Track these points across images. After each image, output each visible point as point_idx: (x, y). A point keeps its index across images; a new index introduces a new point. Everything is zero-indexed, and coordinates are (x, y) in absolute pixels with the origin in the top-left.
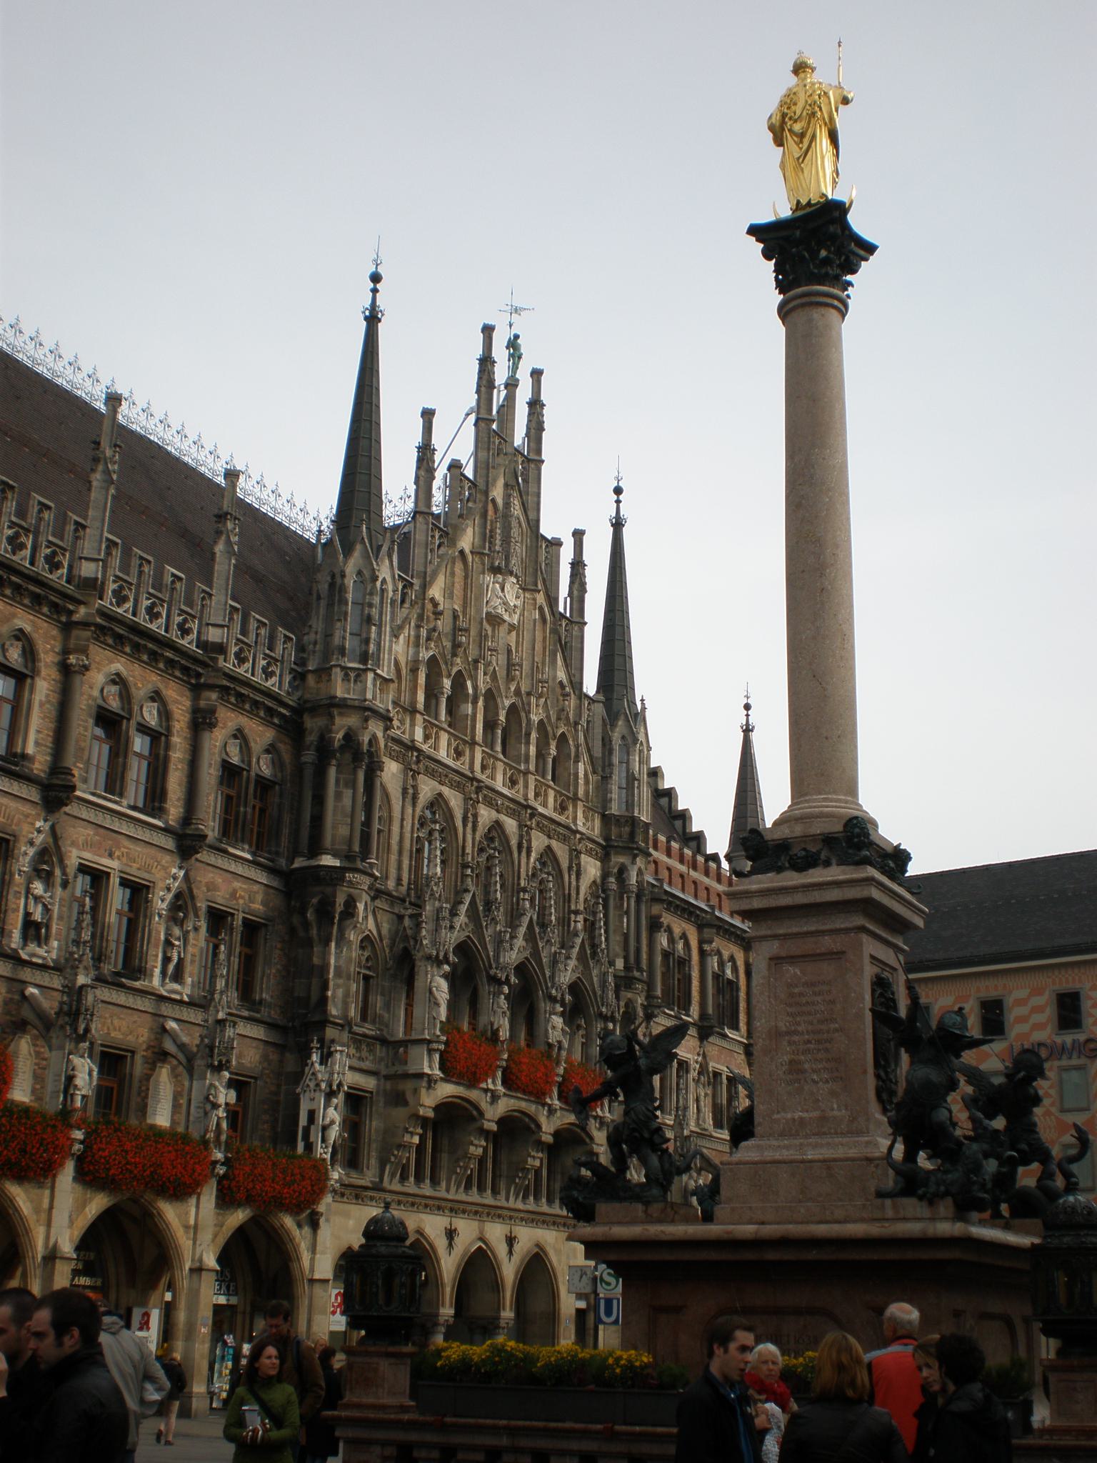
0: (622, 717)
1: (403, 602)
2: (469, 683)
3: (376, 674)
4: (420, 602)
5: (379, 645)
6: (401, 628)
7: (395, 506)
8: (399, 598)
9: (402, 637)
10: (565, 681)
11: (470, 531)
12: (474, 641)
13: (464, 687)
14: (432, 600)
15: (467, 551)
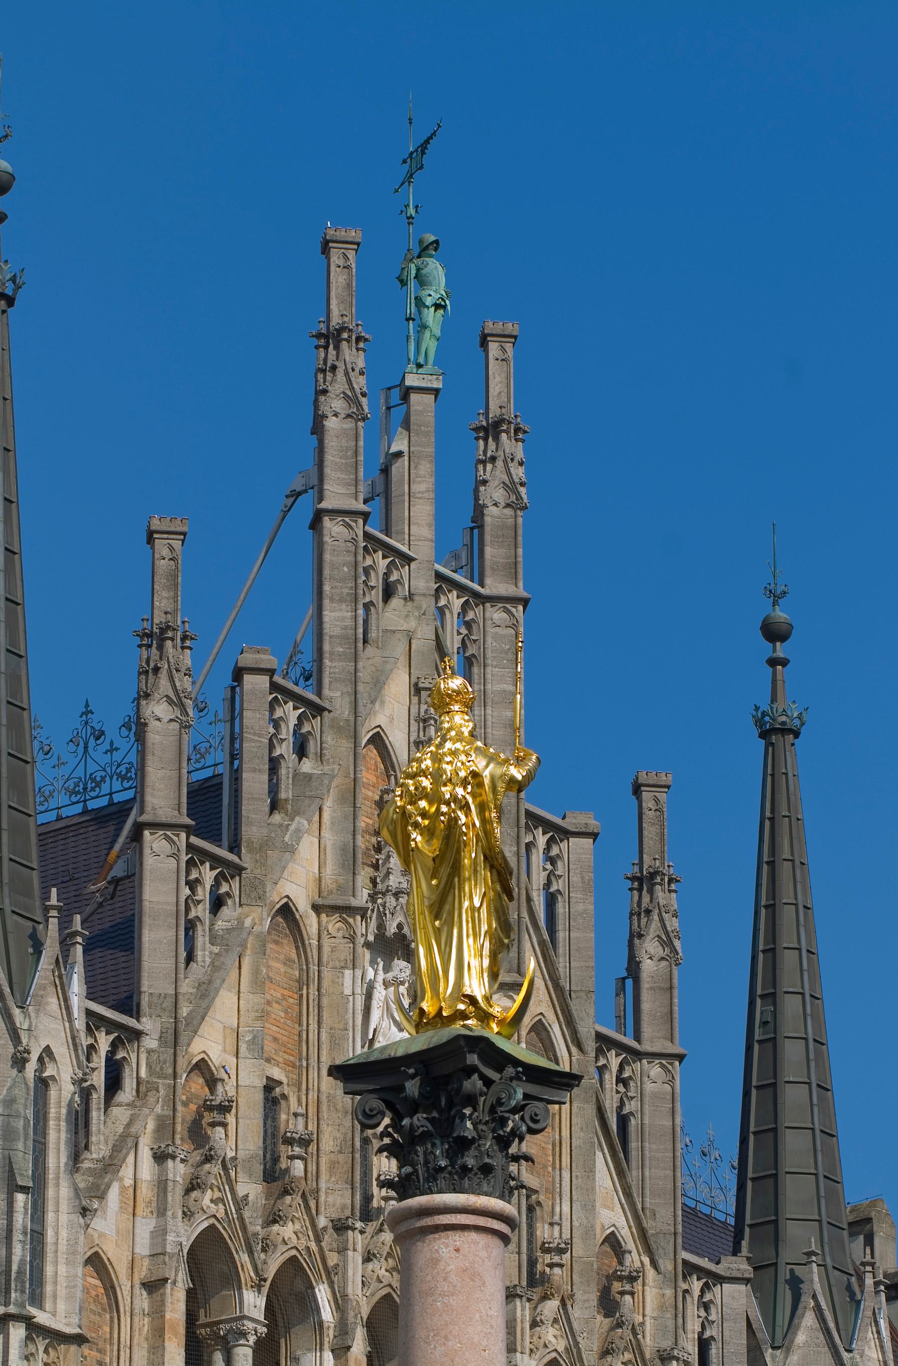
0: (809, 1320)
1: (114, 1083)
2: (322, 1293)
3: (34, 1329)
4: (163, 1085)
5: (37, 1238)
6: (110, 1166)
7: (112, 749)
8: (99, 1079)
9: (113, 1194)
10: (628, 1240)
11: (308, 848)
12: (333, 1165)
13: (309, 1306)
14: (202, 1067)
15: (303, 905)
